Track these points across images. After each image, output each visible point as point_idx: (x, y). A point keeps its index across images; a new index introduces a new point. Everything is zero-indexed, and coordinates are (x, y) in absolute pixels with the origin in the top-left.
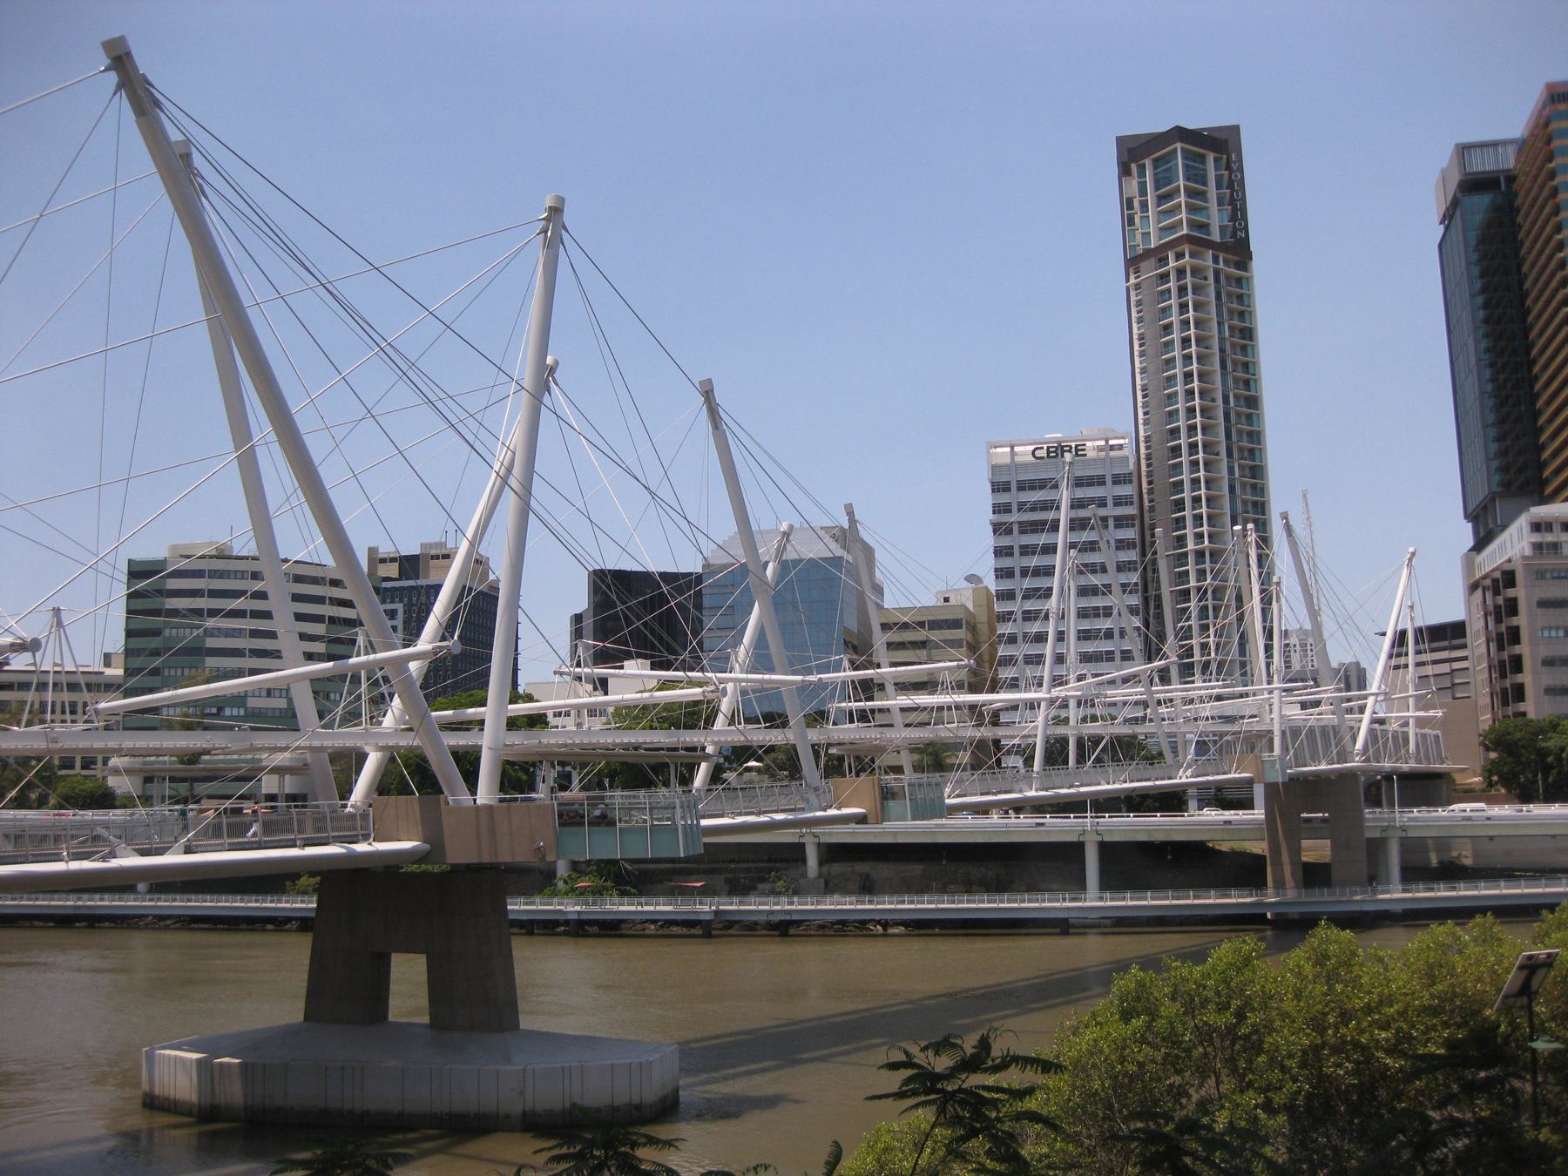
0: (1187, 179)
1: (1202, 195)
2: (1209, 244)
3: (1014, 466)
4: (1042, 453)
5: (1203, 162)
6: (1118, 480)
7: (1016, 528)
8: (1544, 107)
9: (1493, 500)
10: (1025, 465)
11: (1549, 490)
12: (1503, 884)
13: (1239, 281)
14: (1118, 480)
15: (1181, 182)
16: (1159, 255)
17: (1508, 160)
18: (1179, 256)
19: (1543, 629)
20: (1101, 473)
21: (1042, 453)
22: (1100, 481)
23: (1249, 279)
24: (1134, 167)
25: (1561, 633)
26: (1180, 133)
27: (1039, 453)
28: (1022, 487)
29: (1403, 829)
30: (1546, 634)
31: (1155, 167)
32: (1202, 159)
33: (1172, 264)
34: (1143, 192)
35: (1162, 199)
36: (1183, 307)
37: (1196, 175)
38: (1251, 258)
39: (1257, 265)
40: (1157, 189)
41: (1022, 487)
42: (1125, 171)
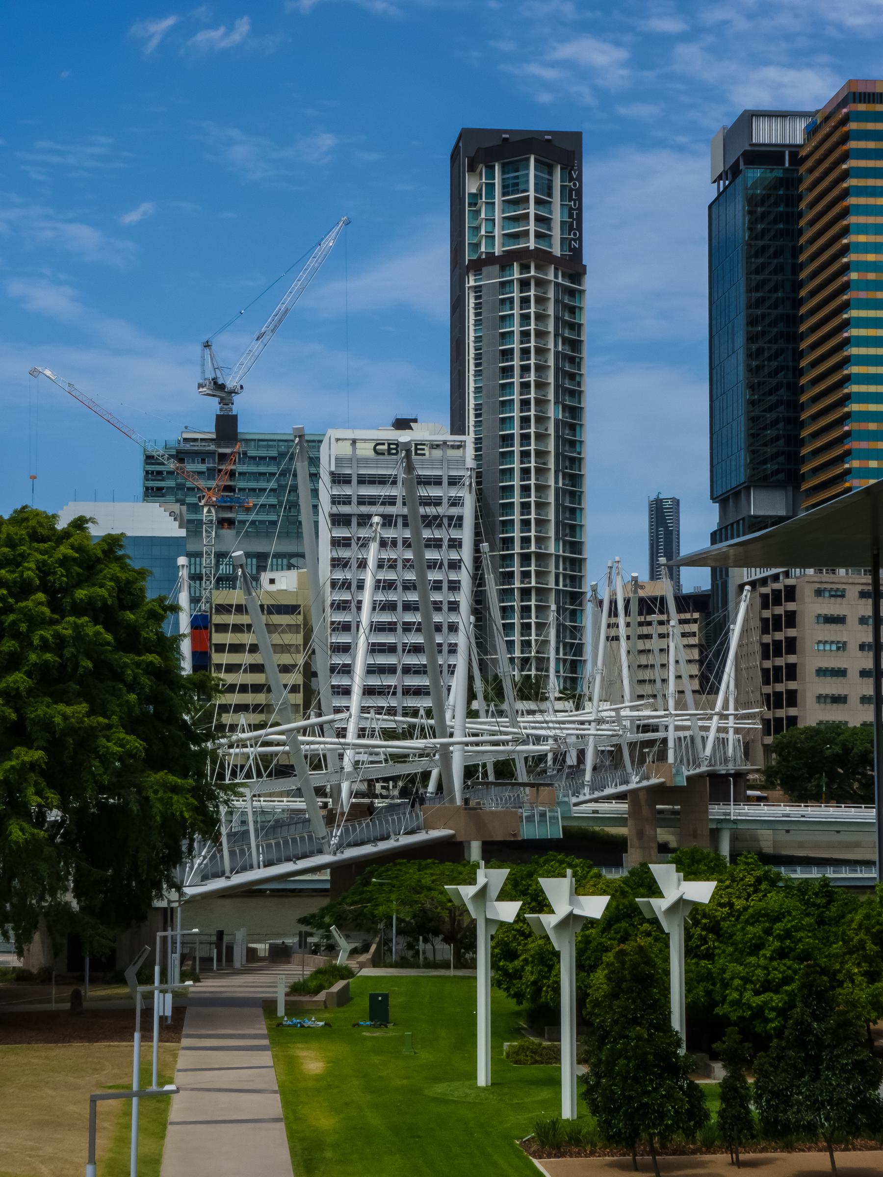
0: (536, 191)
3: (355, 460)
4: (385, 447)
5: (551, 173)
8: (844, 103)
9: (748, 489)
10: (365, 461)
11: (805, 487)
12: (799, 869)
13: (572, 293)
15: (532, 193)
17: (795, 133)
18: (525, 268)
19: (819, 642)
23: (582, 292)
25: (834, 647)
28: (363, 480)
29: (735, 822)
30: (821, 647)
31: (503, 172)
36: (525, 318)
38: (585, 273)
40: (504, 194)
41: (363, 480)
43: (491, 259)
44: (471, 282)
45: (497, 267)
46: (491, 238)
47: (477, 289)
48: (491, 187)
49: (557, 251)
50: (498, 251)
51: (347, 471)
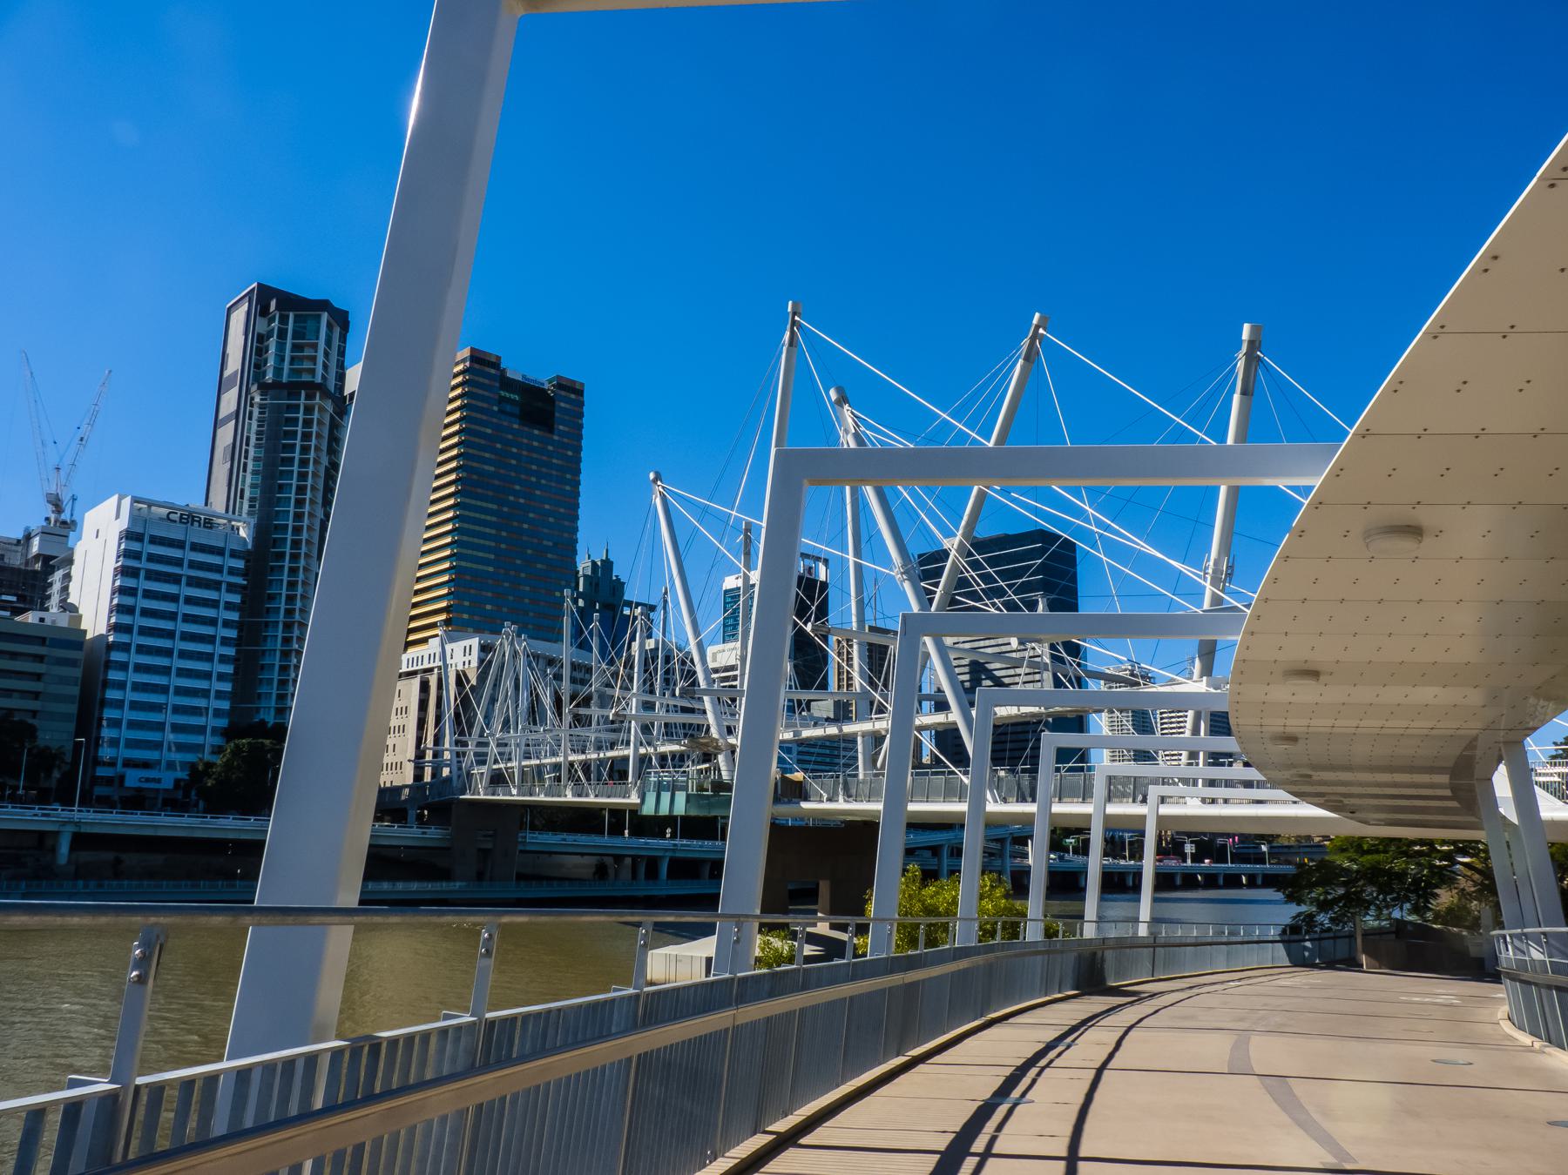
6: (234, 554)
7: (142, 574)
14: (234, 554)
16: (293, 389)
18: (308, 397)
20: (221, 545)
22: (220, 552)
26: (324, 305)
27: (172, 516)
28: (154, 540)
33: (302, 401)
35: (295, 347)
37: (329, 343)
41: (154, 540)
43: (277, 385)
45: (285, 393)
48: (282, 334)
50: (285, 380)
51: (140, 530)
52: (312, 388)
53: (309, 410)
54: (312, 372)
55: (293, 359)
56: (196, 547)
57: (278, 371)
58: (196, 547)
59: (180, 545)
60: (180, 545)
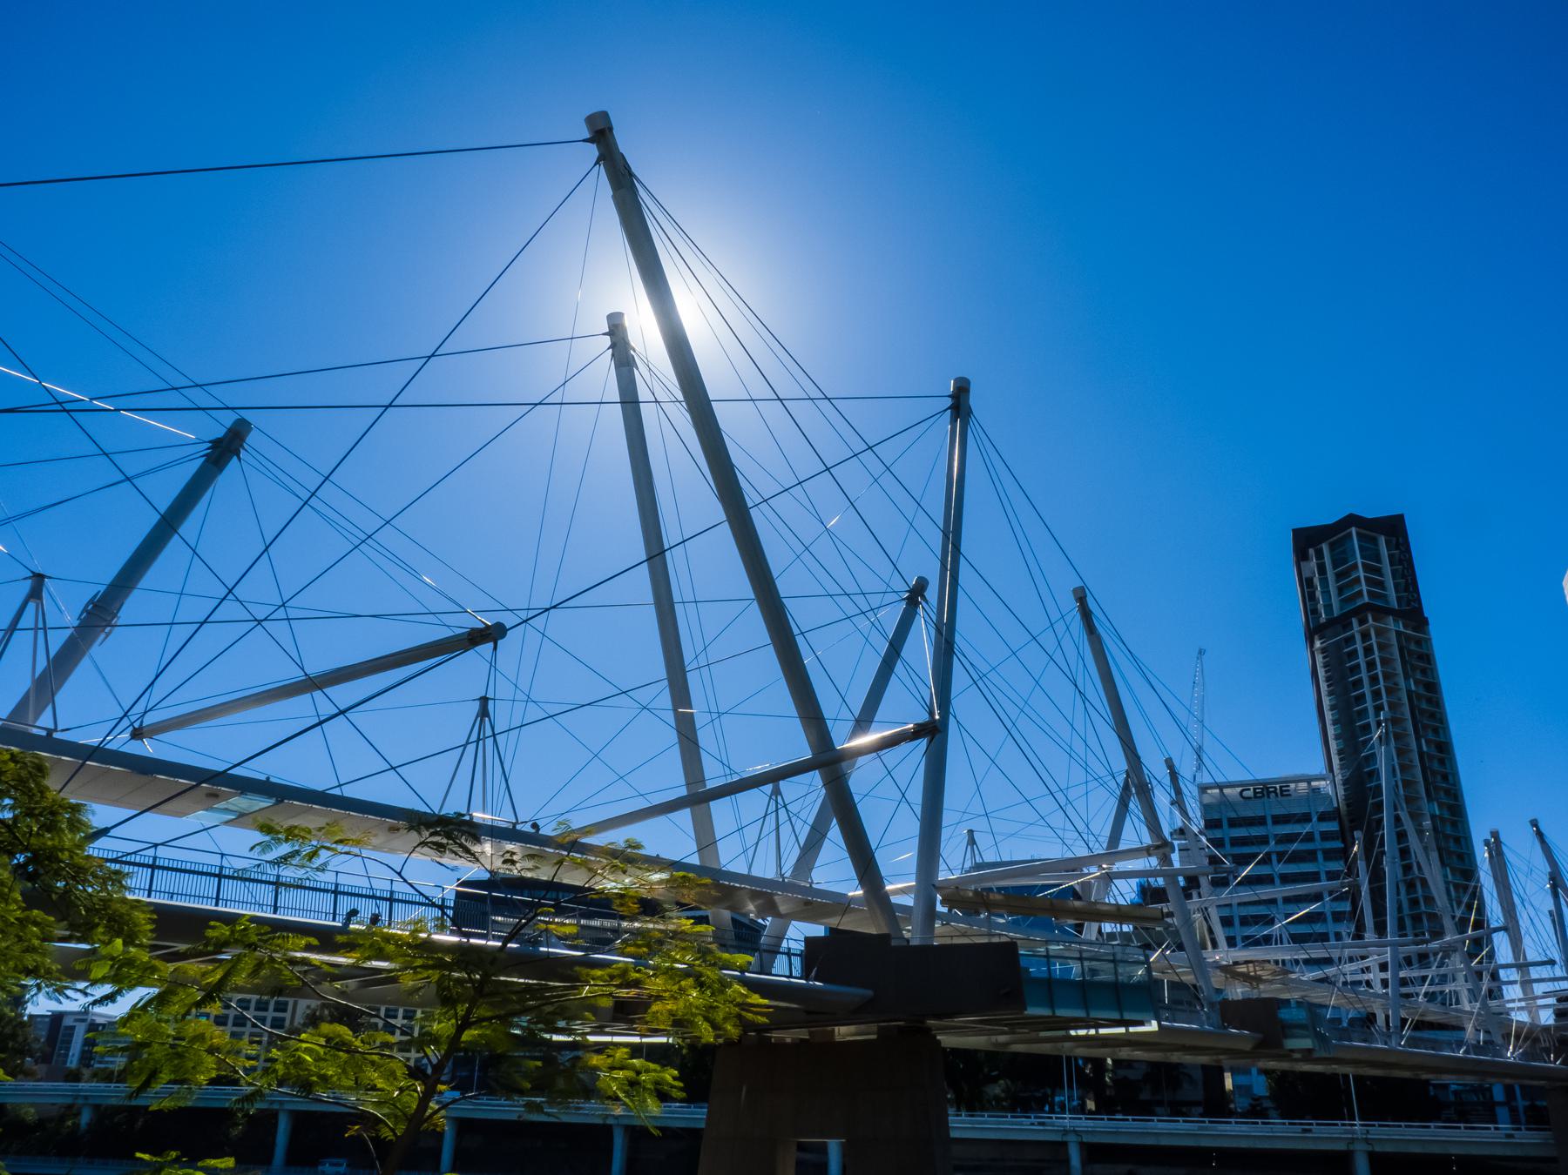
1: (1378, 571)
2: (1389, 611)
4: (1250, 793)
6: (1323, 817)
13: (1418, 642)
14: (1323, 817)
15: (1359, 561)
16: (1343, 622)
18: (1362, 622)
21: (1250, 793)
22: (1306, 818)
24: (1311, 551)
26: (1352, 520)
27: (1246, 794)
28: (1233, 823)
32: (1375, 541)
34: (1322, 569)
35: (1339, 576)
37: (1371, 554)
39: (1431, 628)
41: (1233, 823)
42: (1301, 555)
43: (1332, 622)
44: (1318, 644)
46: (1328, 607)
47: (1323, 650)
49: (1395, 605)
52: (1361, 612)
53: (1365, 636)
54: (1360, 593)
55: (1341, 590)
56: (1278, 820)
57: (1328, 607)
58: (1278, 820)
59: (1261, 821)
60: (1261, 821)
